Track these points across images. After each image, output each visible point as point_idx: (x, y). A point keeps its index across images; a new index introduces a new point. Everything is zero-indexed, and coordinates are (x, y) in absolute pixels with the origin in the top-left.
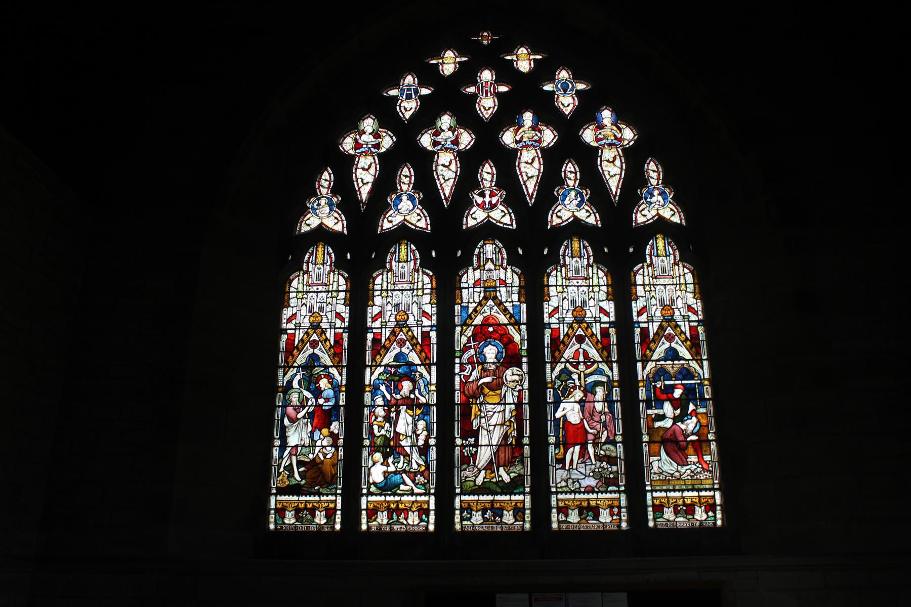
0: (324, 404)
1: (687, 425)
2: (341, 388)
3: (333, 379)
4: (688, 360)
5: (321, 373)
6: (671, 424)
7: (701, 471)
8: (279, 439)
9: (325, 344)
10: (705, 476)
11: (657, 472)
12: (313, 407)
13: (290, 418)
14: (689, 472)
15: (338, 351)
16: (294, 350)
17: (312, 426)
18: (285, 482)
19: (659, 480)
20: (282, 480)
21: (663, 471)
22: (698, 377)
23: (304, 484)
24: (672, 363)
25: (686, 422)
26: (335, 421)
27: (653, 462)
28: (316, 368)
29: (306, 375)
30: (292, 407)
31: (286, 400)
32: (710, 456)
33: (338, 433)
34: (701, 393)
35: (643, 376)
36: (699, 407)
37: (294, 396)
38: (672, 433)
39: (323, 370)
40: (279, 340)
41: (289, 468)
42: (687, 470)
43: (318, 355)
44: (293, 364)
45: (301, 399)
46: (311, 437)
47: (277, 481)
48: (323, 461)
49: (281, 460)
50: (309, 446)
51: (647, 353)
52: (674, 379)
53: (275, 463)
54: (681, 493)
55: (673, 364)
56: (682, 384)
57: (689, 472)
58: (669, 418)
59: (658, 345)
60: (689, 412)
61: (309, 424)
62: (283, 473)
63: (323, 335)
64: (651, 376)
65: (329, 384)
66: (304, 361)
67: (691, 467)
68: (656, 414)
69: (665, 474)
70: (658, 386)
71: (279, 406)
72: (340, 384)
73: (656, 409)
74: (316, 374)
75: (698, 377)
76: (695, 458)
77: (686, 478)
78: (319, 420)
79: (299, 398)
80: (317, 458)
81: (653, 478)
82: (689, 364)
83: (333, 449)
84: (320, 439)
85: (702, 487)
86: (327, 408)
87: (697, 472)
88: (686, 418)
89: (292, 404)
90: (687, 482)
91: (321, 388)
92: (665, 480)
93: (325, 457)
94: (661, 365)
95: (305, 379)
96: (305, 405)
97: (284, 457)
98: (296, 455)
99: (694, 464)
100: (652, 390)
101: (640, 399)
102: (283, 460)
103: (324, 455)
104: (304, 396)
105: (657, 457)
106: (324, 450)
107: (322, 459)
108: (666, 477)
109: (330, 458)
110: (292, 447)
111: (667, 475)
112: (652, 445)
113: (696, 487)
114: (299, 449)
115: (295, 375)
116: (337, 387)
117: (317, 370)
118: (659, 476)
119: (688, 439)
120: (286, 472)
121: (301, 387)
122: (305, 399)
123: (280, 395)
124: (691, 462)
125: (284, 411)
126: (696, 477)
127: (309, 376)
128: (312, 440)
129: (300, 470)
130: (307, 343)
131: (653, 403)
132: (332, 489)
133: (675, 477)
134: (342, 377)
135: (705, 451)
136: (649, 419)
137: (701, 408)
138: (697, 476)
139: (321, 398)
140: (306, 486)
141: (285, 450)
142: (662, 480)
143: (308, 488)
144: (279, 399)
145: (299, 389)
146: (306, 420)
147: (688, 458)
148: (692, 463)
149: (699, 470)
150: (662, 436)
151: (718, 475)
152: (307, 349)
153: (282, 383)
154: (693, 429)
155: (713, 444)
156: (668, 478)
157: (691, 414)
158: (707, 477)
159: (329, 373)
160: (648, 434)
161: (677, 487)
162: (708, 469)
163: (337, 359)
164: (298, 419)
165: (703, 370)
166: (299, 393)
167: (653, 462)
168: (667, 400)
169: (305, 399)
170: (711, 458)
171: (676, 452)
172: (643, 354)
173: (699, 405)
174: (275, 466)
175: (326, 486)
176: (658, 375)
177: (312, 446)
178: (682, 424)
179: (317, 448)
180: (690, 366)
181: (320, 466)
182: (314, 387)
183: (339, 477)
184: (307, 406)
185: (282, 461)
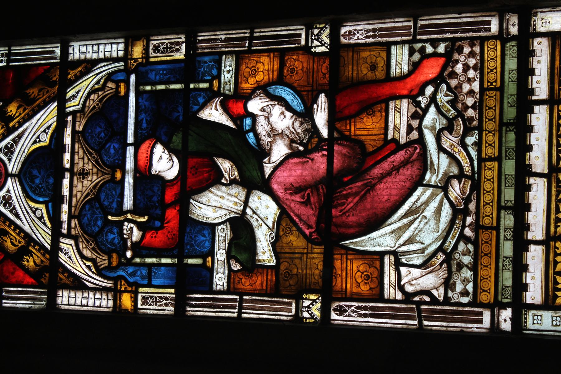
1: (274, 133)
4: (62, 115)
6: (266, 199)
7: (449, 88)
10: (471, 74)
11: (443, 273)
14: (448, 141)
19: (474, 268)
21: (440, 249)
22: (117, 83)
24: (67, 175)
25: (265, 140)
27: (401, 288)
32: (393, 48)
34: (171, 71)
35: (103, 290)
36: (216, 83)
38: (297, 198)
42: (441, 149)
51: (31, 263)
52: (118, 175)
54: (532, 180)
55: (71, 170)
56: (137, 145)
57: (448, 141)
58: (246, 203)
59: (12, 222)
60: (230, 124)
64: (103, 261)
67: (433, 128)
68: (229, 256)
69: (451, 241)
70: (136, 235)
73: (212, 253)
75: (117, 83)
76: (398, 110)
77: (474, 154)
81: (465, 293)
82: (74, 113)
85: (512, 89)
87: (453, 103)
88: (251, 137)
90: (489, 152)
92: (475, 243)
94: (70, 217)
99: (422, 118)
100: (149, 260)
101: (170, 310)
105: (386, 268)
108: (467, 240)
111: (455, 233)
112: (338, 284)
113: (511, 113)
118: (460, 266)
119: (325, 133)
124: (410, 129)
126: (470, 113)
131: (191, 261)
133: (467, 201)
135: (373, 67)
136: (246, 283)
137: (218, 77)
138: (466, 107)
142: (476, 257)
147: (394, 140)
148: (415, 123)
149: (442, 98)
150: (308, 239)
151: (467, 18)
154: (288, 114)
155: (349, 34)
156: (468, 232)
157: (237, 119)
158: (472, 62)
160: (298, 298)
161: (509, 194)
162: (442, 61)
165: (99, 61)
167: (401, 288)
168: (185, 209)
170: (403, 43)
171: (371, 187)
172: (31, 280)
173: (211, 82)
176: (102, 230)
178: (268, 154)
180: (82, 111)
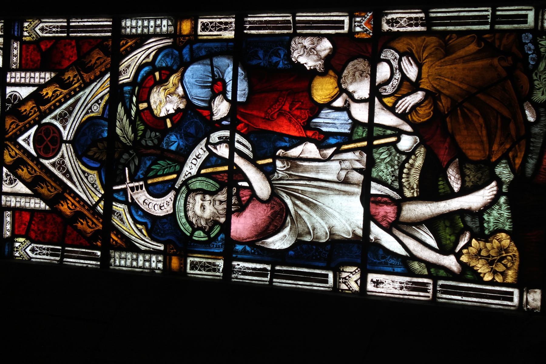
0: (229, 96)
2: (181, 35)
3: (155, 69)
5: (133, 113)
8: (337, 272)
9: (49, 100)
12: (237, 137)
13: (267, 227)
15: (71, 54)
16: (61, 213)
17: (300, 141)
18: (501, 249)
20: (490, 262)
23: (513, 170)
26: (289, 54)
28: (118, 131)
29: (137, 168)
30: (234, 219)
31: (211, 241)
33: (329, 37)
37: (198, 211)
39: (124, 105)
40: (28, 264)
41: (448, 237)
43: (81, 125)
44: (99, 213)
45: (209, 185)
46: (338, 145)
47: (492, 283)
48: (428, 95)
49: (416, 265)
50: (369, 150)
53: (422, 287)
61: (295, 152)
62: (464, 259)
63: (23, 109)
65: (167, 80)
66: (94, 176)
71: (228, 269)
72: (168, 42)
74: (135, 131)
78: (281, 114)
79: (204, 192)
80: (415, 118)
83: (388, 54)
84: (346, 109)
86: (243, 87)
89: (222, 220)
91: (178, 110)
93: (414, 87)
95: (149, 169)
96: (226, 168)
97: (401, 251)
98: (399, 204)
102: (413, 257)
103: (404, 91)
104: (198, 174)
106: (389, 89)
107: (418, 96)
109: (420, 66)
110: (368, 217)
114: (376, 189)
115: (133, 206)
116: (180, 50)
117: (123, 129)
120: (462, 244)
121: (169, 187)
122: (210, 170)
123: (194, 266)
125: (244, 251)
127: (141, 156)
128: (348, 138)
129: (456, 187)
130: (43, 167)
132: (537, 51)
134: (149, 36)
139: (210, 108)
140: (518, 161)
141: (377, 245)
143: (528, 152)
144: (204, 267)
145: (178, 191)
146: (279, 164)
152: (61, 166)
153: (154, 258)
159: (133, 83)
163: (96, 56)
164: (274, 194)
166: (190, 191)
169: (210, 170)
174: (435, 291)
175: (524, 78)
177: (370, 138)
179: (376, 120)
181: (444, 104)
182: (173, 138)
183: (492, 24)
184: (230, 162)
185: (420, 260)
